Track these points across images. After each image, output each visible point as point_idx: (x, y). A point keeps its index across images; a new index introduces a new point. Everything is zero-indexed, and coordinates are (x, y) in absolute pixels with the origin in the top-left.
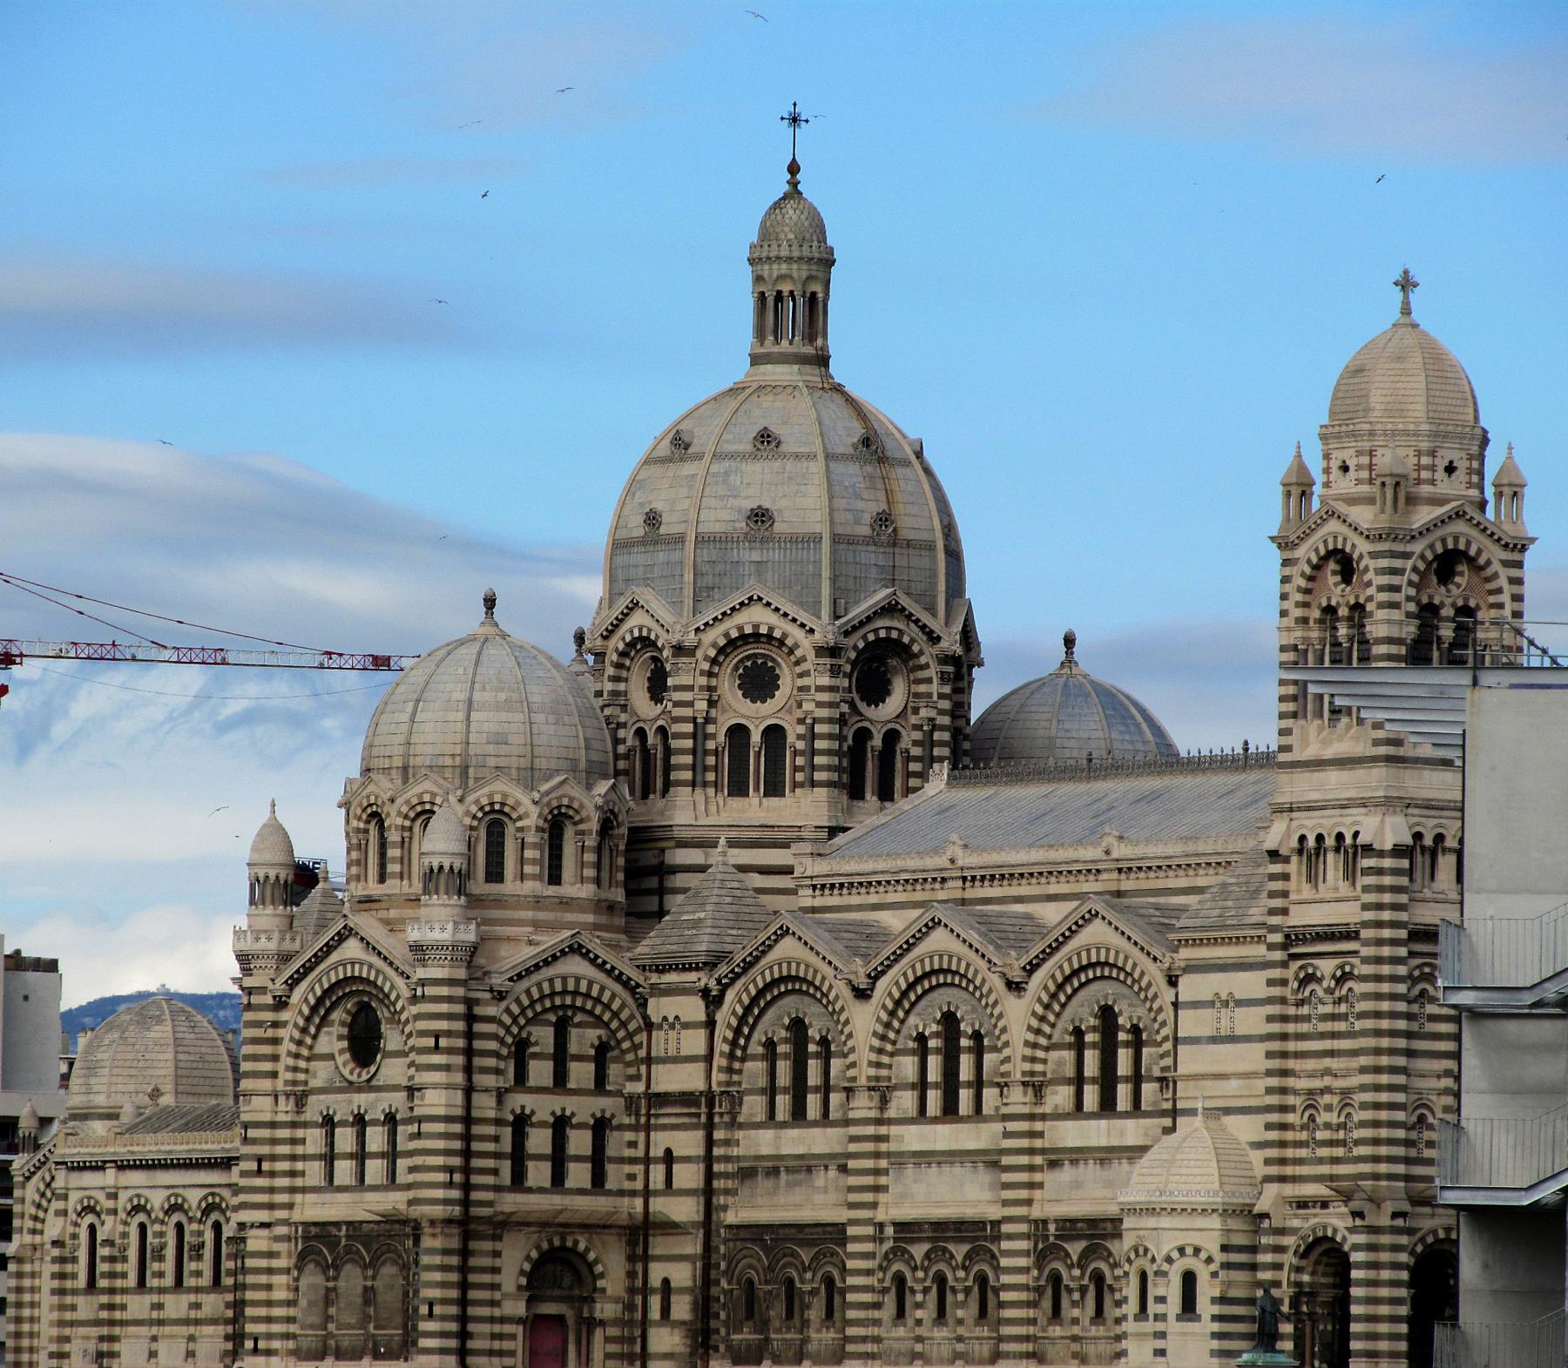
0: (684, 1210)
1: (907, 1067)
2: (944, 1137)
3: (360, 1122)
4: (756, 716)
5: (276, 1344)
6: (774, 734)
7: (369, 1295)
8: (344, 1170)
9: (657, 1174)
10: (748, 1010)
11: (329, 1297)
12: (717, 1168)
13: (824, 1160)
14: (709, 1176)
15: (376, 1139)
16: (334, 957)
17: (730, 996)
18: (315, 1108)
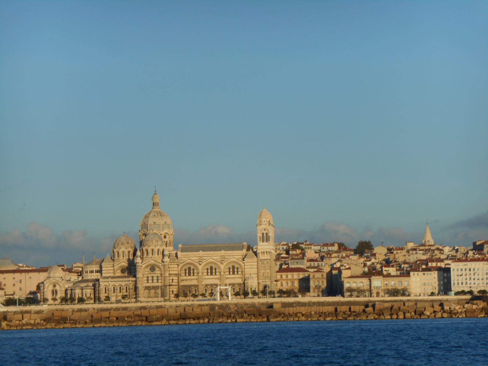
0: (177, 284)
1: (206, 271)
2: (211, 277)
3: (153, 277)
4: (165, 240)
5: (142, 297)
6: (167, 241)
7: (155, 292)
8: (150, 281)
9: (171, 281)
10: (183, 266)
11: (149, 293)
12: (179, 280)
13: (194, 279)
14: (178, 281)
15: (155, 278)
16: (149, 262)
17: (181, 266)
18: (145, 276)
